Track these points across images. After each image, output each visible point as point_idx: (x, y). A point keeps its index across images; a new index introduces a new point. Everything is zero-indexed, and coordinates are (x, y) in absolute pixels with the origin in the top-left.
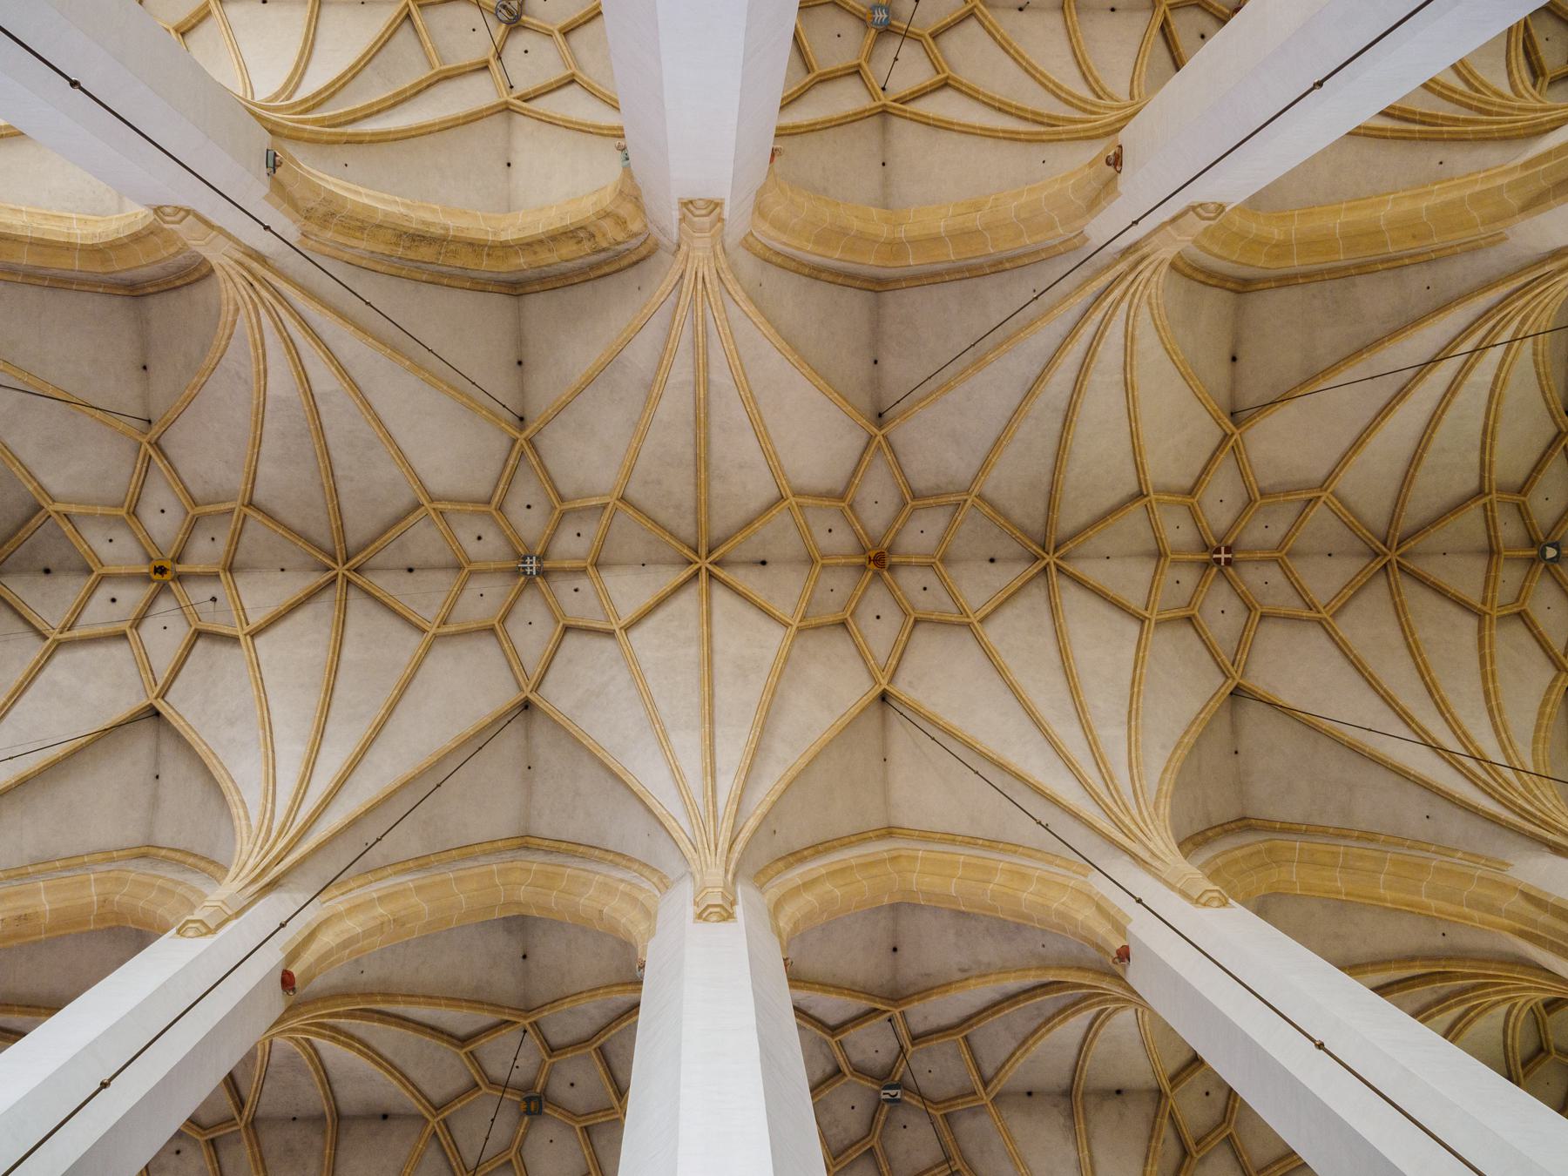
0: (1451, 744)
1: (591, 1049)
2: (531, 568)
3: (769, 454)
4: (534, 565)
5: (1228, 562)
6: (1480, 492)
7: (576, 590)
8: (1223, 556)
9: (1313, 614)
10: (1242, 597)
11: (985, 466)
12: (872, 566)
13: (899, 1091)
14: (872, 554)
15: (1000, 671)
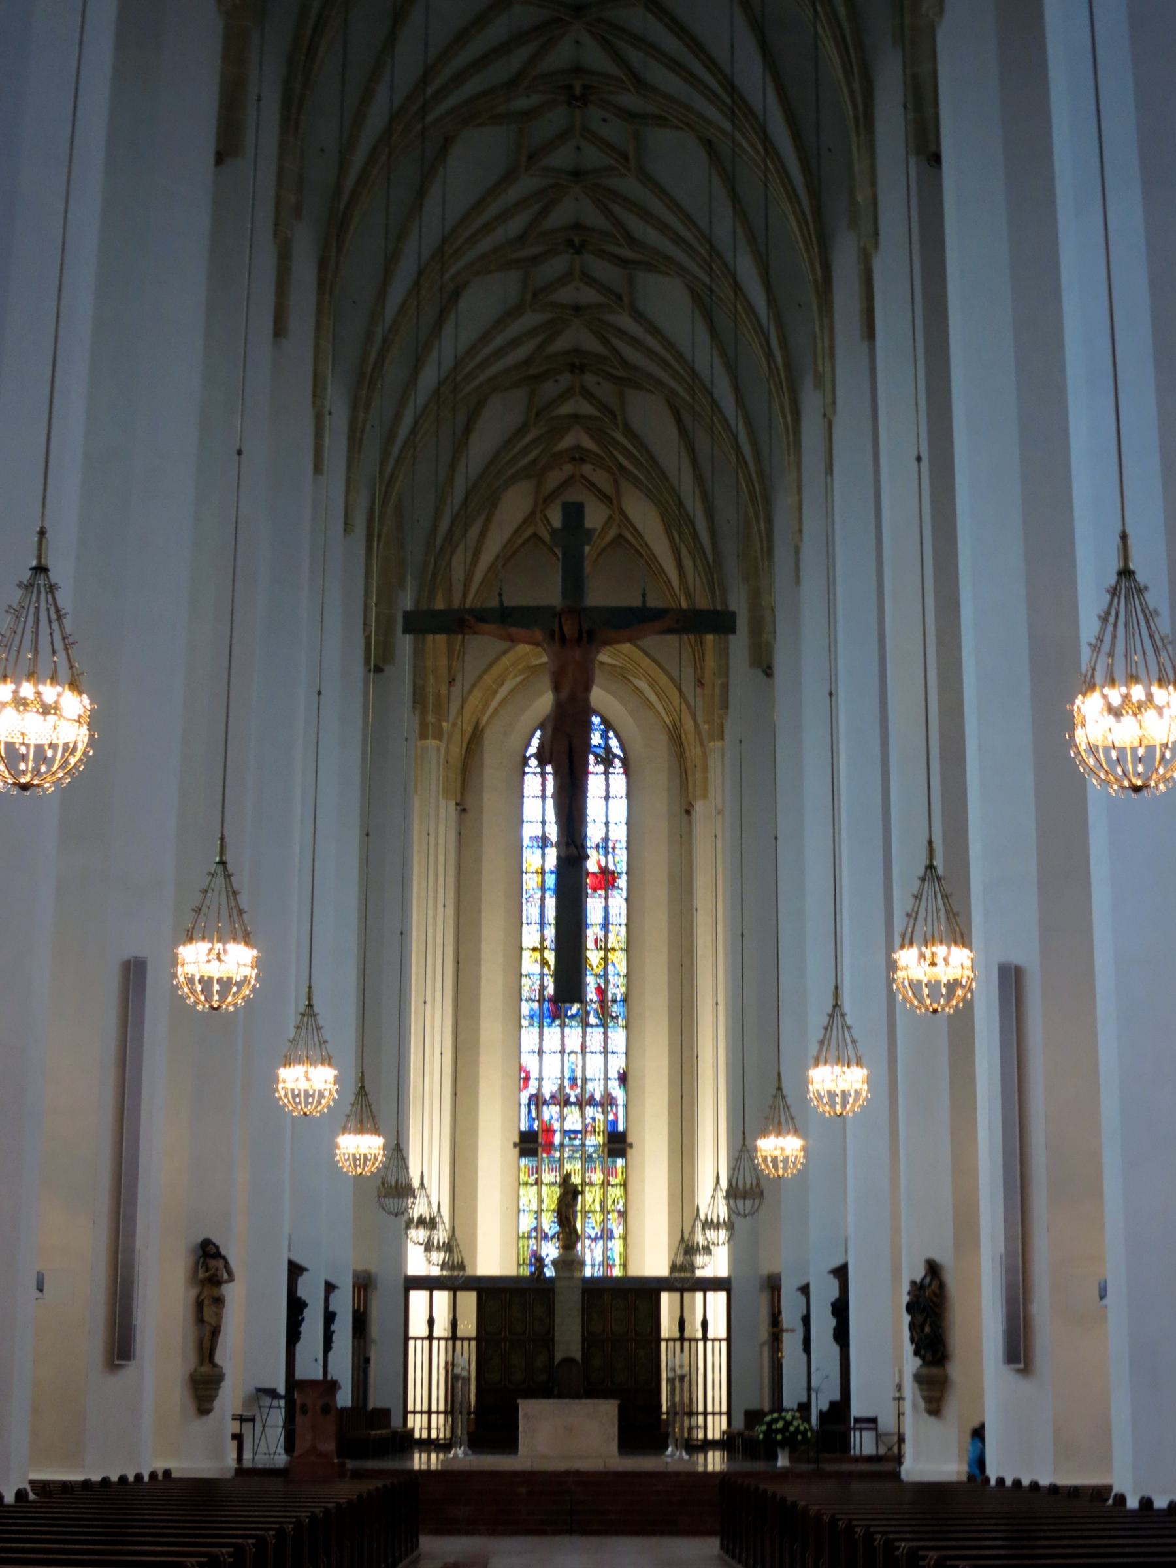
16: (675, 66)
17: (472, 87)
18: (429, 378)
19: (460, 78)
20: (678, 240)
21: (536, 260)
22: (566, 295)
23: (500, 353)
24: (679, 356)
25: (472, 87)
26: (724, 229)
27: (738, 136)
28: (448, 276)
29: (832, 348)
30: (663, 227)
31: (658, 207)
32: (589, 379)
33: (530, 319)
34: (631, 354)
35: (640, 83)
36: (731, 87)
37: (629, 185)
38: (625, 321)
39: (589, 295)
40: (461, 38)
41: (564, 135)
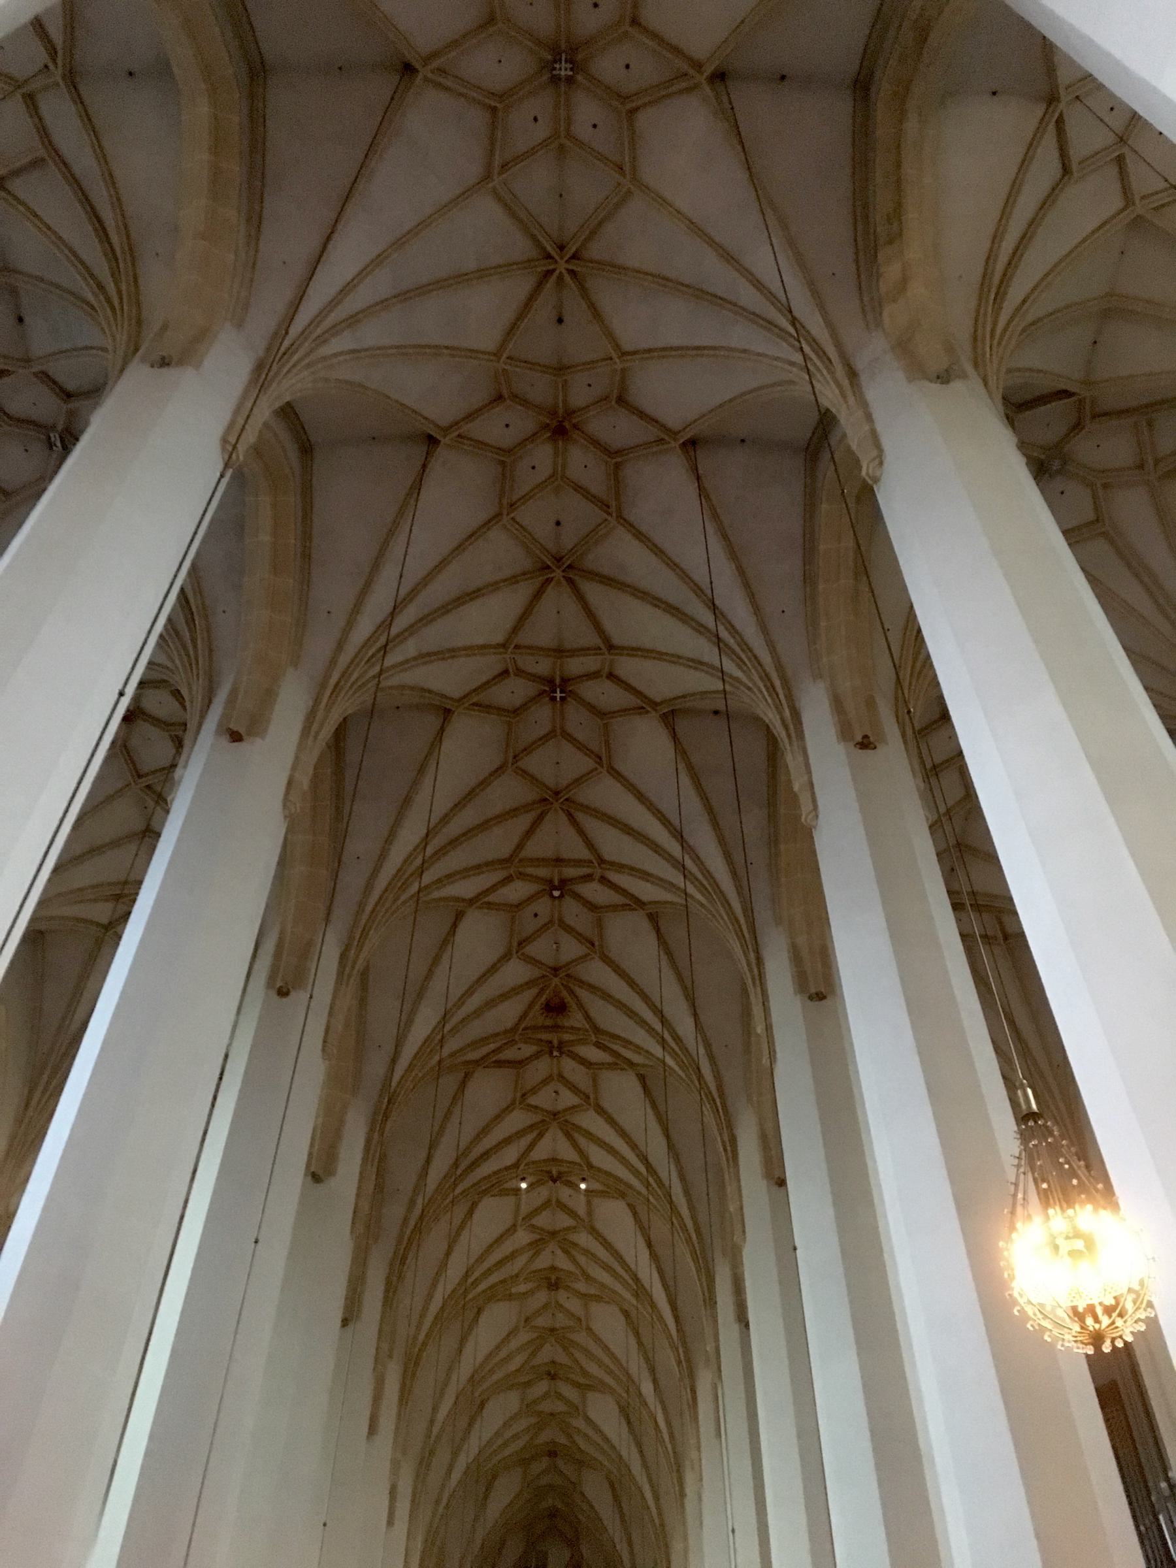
0: (401, 622)
1: (42, 153)
2: (560, 69)
3: (666, 352)
4: (563, 73)
5: (553, 699)
6: (602, 861)
7: (536, 119)
8: (558, 695)
9: (511, 760)
10: (525, 706)
11: (640, 536)
12: (555, 424)
13: (60, 448)
14: (567, 424)
15: (460, 548)
16: (607, 1268)
17: (494, 1278)
18: (462, 1462)
19: (489, 1272)
20: (610, 1373)
21: (528, 1384)
22: (546, 1407)
23: (506, 1444)
24: (613, 1447)
25: (494, 1278)
26: (636, 1366)
27: (640, 1306)
28: (477, 1394)
29: (699, 1442)
30: (600, 1363)
31: (599, 1352)
32: (560, 1463)
33: (523, 1424)
34: (582, 1444)
35: (588, 1278)
36: (636, 1279)
37: (581, 1338)
38: (579, 1423)
39: (560, 1407)
40: (489, 1249)
41: (545, 1307)
